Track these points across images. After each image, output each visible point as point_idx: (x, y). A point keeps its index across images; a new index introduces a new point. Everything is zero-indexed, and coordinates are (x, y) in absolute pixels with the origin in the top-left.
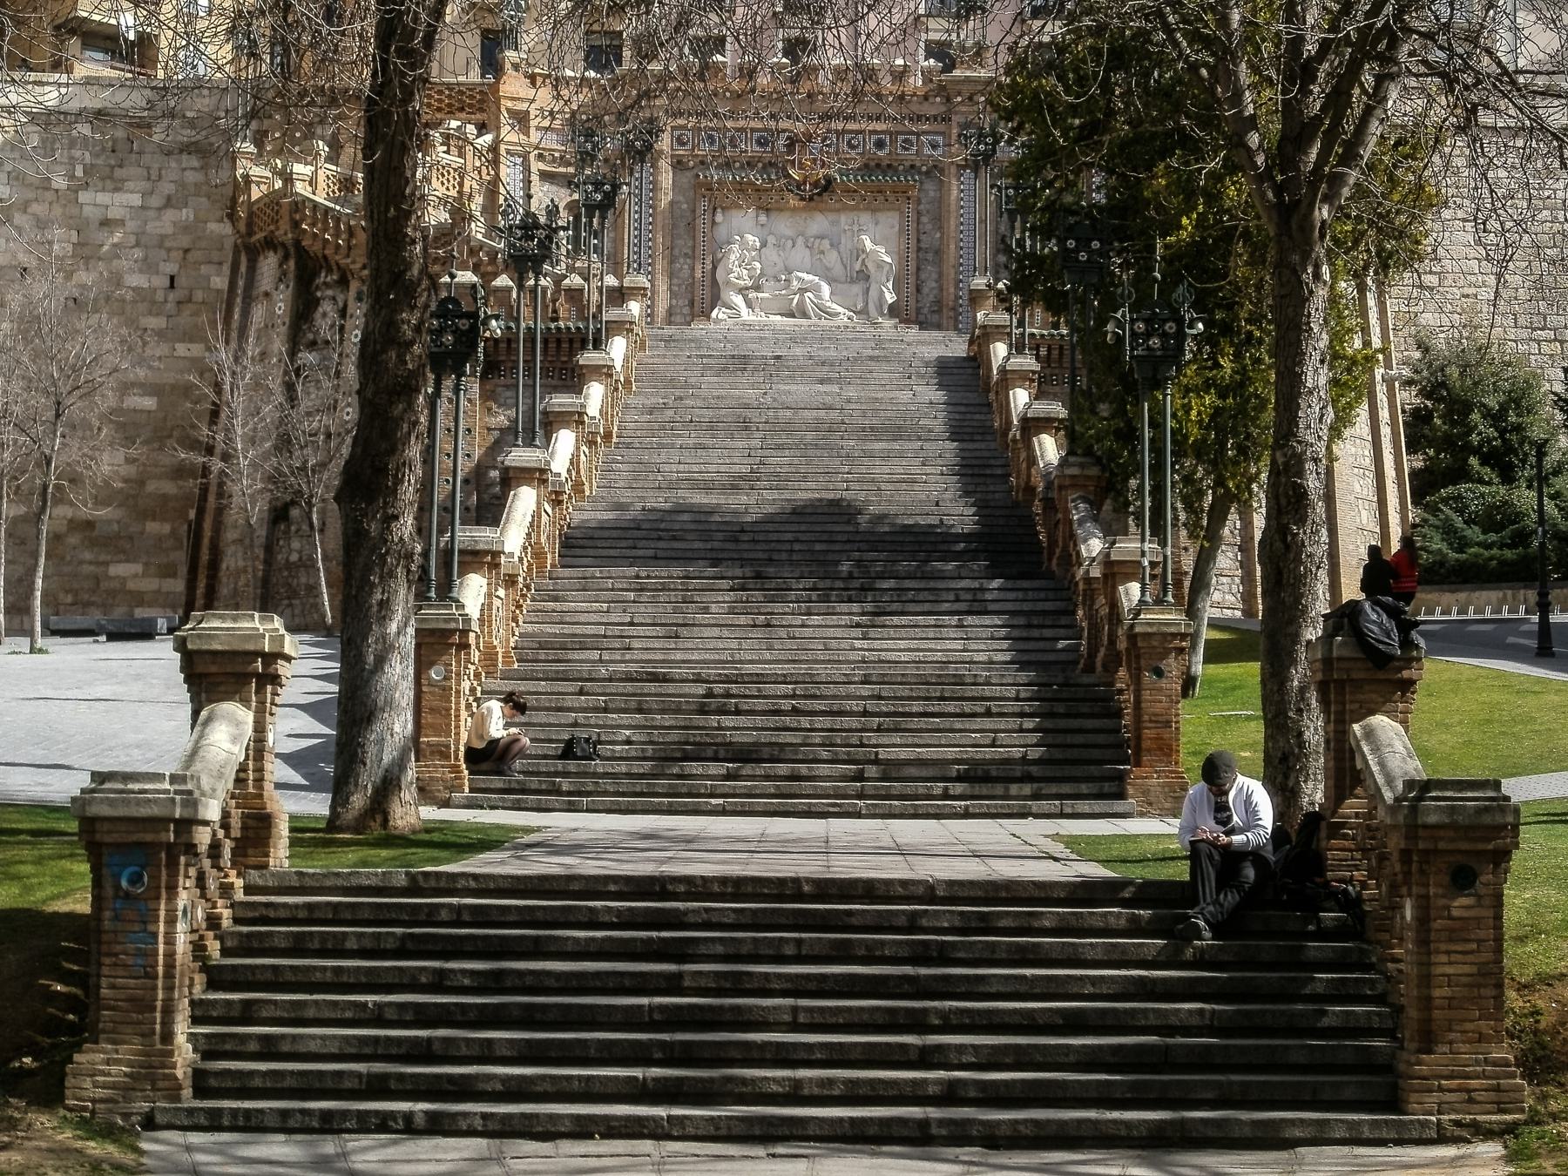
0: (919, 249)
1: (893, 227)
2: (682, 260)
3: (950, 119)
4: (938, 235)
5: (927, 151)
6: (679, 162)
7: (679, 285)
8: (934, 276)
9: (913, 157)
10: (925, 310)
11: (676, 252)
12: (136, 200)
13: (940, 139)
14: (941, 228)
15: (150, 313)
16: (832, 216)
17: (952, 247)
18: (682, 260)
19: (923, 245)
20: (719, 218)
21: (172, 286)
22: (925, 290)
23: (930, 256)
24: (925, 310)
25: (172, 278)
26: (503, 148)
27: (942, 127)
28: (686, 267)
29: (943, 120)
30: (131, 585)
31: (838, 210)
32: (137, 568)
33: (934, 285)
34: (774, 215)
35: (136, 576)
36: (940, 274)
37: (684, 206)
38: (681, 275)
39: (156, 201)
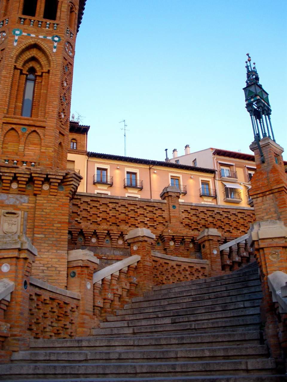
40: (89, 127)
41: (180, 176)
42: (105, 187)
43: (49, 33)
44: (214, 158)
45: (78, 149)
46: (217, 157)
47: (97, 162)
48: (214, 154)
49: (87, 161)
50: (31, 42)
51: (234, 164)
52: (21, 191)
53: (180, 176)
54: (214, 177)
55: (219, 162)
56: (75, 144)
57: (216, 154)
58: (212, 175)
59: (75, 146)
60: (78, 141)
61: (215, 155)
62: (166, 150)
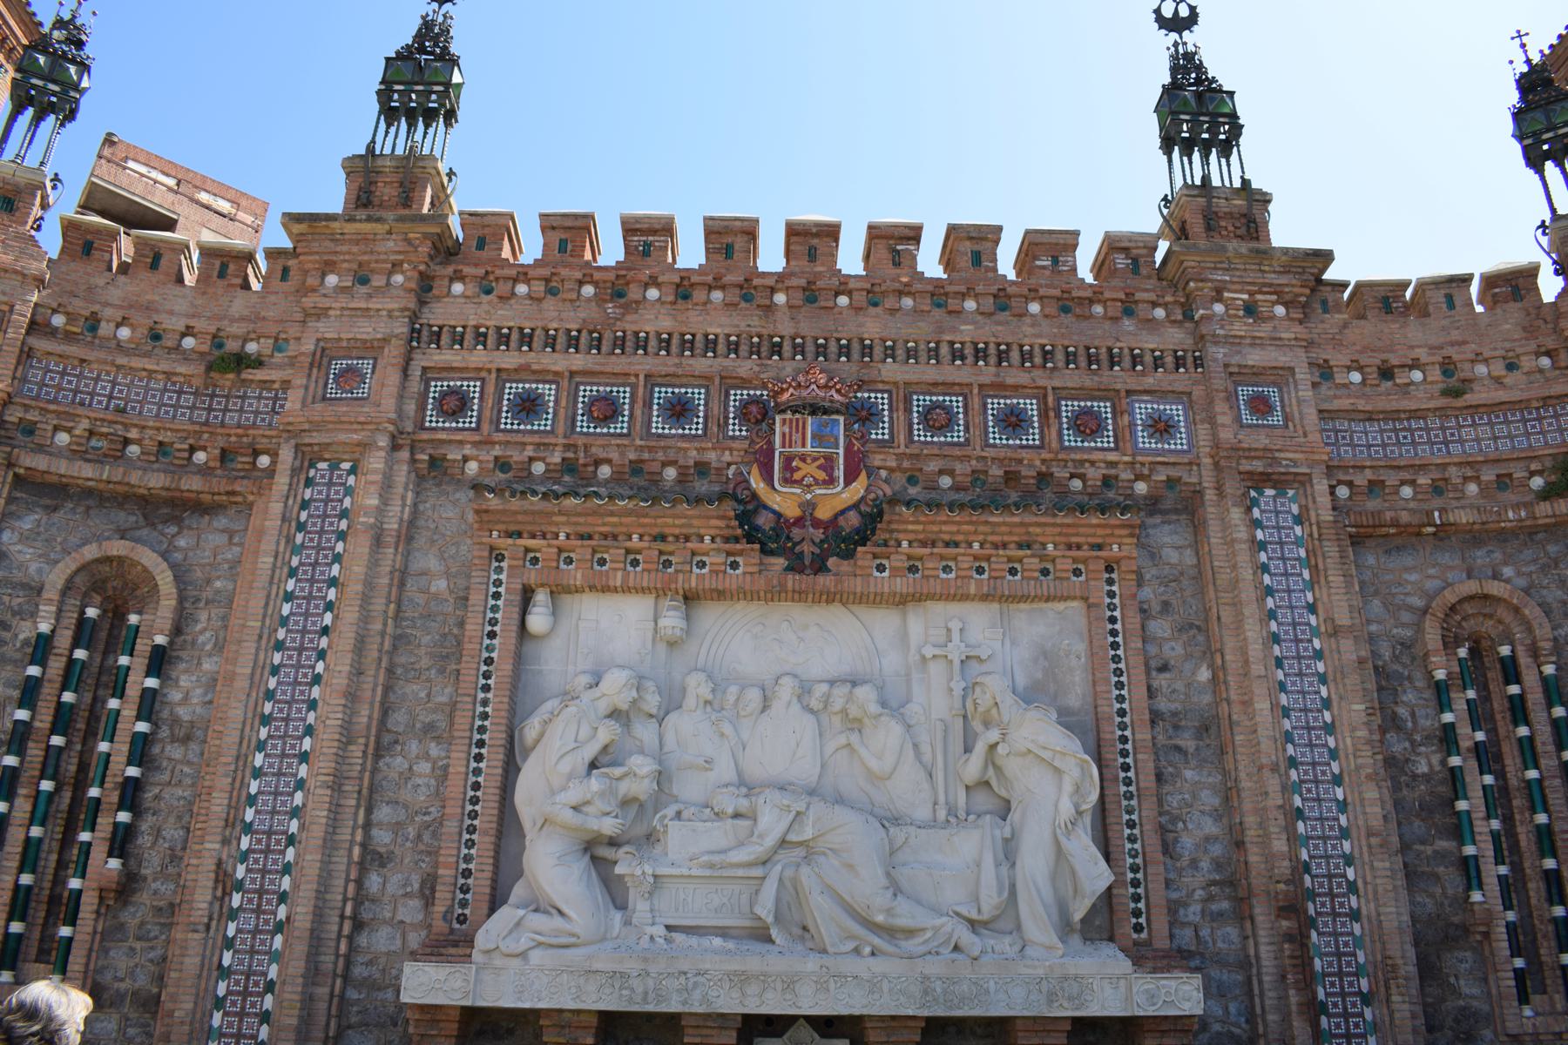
0: (1155, 717)
2: (414, 747)
3: (1199, 362)
4: (1204, 675)
5: (1144, 440)
7: (397, 827)
8: (1209, 799)
9: (1112, 457)
10: (1193, 912)
11: (398, 720)
13: (1176, 411)
14: (1211, 653)
16: (884, 622)
17: (1262, 705)
18: (414, 747)
19: (1163, 705)
20: (538, 621)
22: (1187, 842)
23: (1188, 742)
24: (1193, 912)
27: (1181, 380)
28: (424, 767)
29: (1179, 362)
31: (901, 601)
33: (1211, 827)
34: (711, 616)
36: (1229, 794)
37: (441, 585)
38: (406, 795)
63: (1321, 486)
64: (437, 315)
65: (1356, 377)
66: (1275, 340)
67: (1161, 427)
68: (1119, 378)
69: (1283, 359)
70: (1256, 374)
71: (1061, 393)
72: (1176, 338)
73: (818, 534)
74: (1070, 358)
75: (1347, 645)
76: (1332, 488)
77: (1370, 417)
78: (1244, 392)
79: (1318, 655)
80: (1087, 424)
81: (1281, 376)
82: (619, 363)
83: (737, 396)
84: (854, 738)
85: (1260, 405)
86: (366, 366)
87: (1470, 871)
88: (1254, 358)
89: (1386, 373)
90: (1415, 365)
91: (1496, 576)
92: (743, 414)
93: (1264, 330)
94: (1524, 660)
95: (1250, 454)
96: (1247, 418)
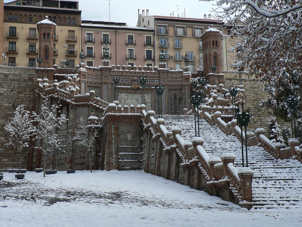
1: (150, 96)
3: (160, 77)
5: (156, 83)
6: (112, 84)
12: (6, 90)
13: (158, 81)
15: (9, 111)
19: (155, 99)
21: (13, 106)
22: (156, 107)
23: (157, 101)
25: (13, 104)
26: (81, 81)
30: (6, 163)
32: (7, 160)
35: (7, 161)
39: (9, 90)
40: (81, 11)
41: (133, 34)
42: (91, 44)
43: (48, 43)
44: (155, 22)
45: (76, 24)
46: (156, 21)
47: (87, 30)
48: (155, 20)
49: (81, 30)
50: (45, 45)
51: (167, 25)
52: (46, 72)
53: (133, 34)
54: (154, 34)
55: (157, 24)
56: (75, 21)
57: (156, 20)
58: (153, 33)
59: (75, 22)
60: (76, 19)
61: (155, 20)
62: (139, 10)
63: (166, 86)
64: (111, 74)
65: (170, 78)
66: (165, 76)
67: (157, 82)
68: (154, 78)
69: (165, 77)
70: (163, 78)
71: (151, 79)
72: (158, 76)
73: (135, 89)
74: (151, 77)
75: (166, 96)
76: (167, 86)
77: (170, 81)
78: (162, 79)
79: (165, 97)
80: (152, 82)
81: (165, 78)
82: (123, 77)
83: (130, 80)
84: (138, 101)
85: (163, 81)
86: (107, 77)
87: (172, 109)
88: (163, 77)
89: (172, 78)
90: (174, 78)
91: (177, 92)
92: (131, 81)
93: (164, 75)
94: (177, 97)
95: (162, 84)
96: (162, 81)
